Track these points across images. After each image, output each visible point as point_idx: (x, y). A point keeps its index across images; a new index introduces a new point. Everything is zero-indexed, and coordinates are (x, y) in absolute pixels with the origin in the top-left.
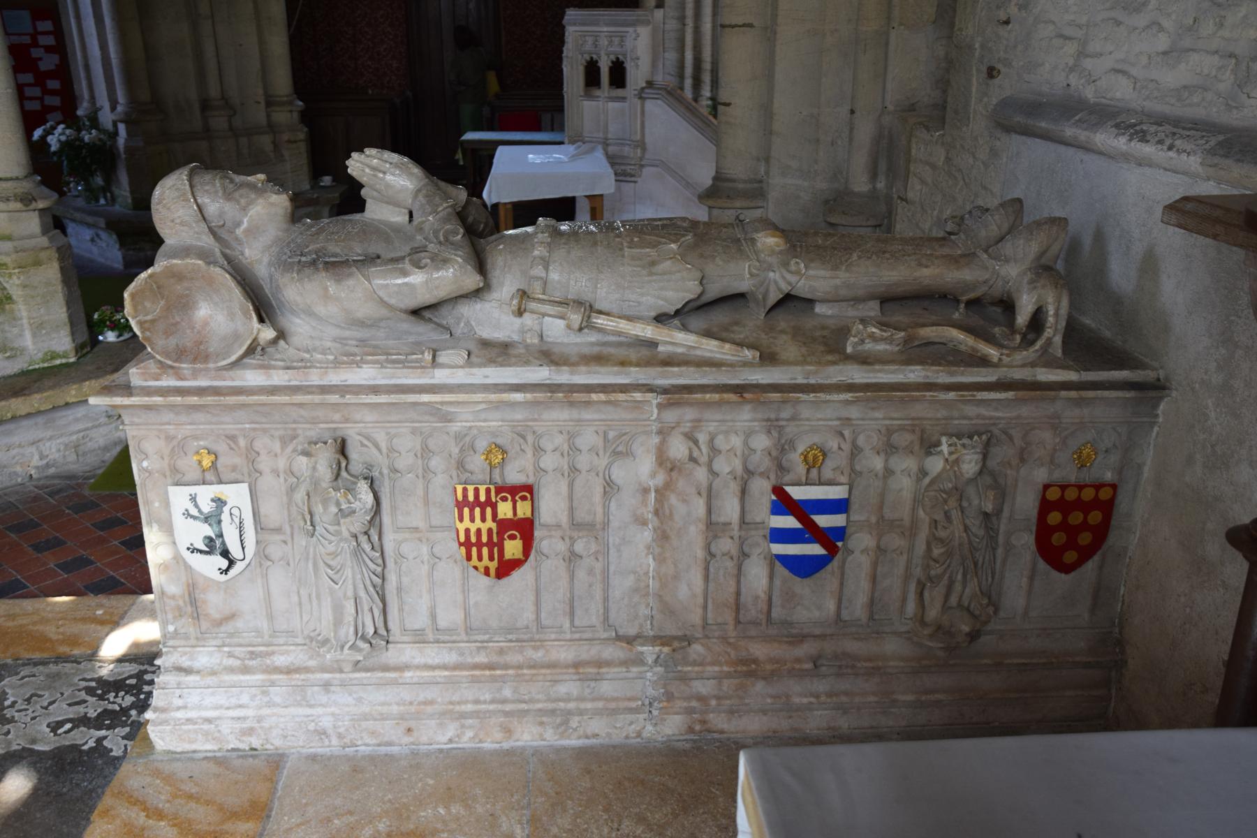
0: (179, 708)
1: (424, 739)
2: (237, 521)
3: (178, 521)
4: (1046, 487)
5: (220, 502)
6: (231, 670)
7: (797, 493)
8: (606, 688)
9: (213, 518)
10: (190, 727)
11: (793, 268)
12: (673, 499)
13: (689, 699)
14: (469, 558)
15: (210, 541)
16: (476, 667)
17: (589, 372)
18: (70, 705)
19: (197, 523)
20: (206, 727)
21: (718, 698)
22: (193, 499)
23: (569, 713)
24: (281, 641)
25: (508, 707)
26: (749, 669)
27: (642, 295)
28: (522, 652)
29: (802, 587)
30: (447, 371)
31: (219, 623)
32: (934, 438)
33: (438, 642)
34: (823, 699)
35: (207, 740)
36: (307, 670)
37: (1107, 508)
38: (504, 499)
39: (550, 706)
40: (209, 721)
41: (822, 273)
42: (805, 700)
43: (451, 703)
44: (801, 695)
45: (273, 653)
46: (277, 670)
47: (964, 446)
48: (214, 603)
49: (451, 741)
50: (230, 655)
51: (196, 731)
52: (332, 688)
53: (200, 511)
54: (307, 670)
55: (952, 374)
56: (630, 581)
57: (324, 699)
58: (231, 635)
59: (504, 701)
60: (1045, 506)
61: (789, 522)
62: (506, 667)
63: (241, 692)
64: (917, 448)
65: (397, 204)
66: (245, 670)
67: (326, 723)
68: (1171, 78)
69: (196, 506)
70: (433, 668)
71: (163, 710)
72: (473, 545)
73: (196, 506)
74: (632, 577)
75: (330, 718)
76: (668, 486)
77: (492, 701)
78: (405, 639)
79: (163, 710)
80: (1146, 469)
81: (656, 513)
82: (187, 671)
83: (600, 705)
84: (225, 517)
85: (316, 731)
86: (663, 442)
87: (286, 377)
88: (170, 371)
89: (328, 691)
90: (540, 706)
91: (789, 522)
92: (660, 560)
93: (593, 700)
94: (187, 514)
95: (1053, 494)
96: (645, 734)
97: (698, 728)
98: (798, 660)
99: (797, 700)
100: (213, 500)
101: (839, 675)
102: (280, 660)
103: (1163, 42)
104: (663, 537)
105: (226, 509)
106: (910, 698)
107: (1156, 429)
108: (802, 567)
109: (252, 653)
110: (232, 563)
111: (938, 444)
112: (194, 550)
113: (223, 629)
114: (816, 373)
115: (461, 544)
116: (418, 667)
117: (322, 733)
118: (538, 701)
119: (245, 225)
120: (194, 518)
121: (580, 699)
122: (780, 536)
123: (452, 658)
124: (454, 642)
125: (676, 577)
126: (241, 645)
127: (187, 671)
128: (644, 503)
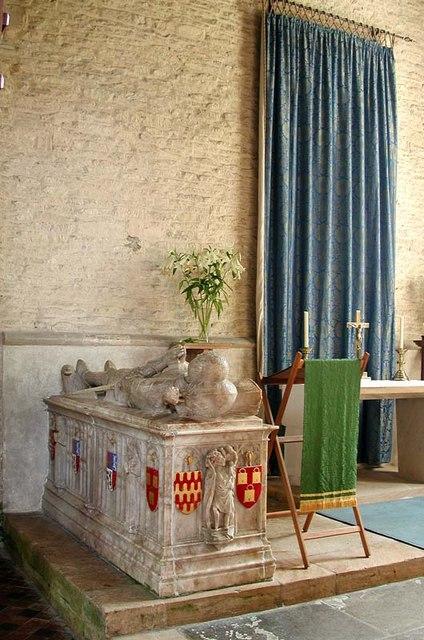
68: (91, 323)
103: (84, 315)
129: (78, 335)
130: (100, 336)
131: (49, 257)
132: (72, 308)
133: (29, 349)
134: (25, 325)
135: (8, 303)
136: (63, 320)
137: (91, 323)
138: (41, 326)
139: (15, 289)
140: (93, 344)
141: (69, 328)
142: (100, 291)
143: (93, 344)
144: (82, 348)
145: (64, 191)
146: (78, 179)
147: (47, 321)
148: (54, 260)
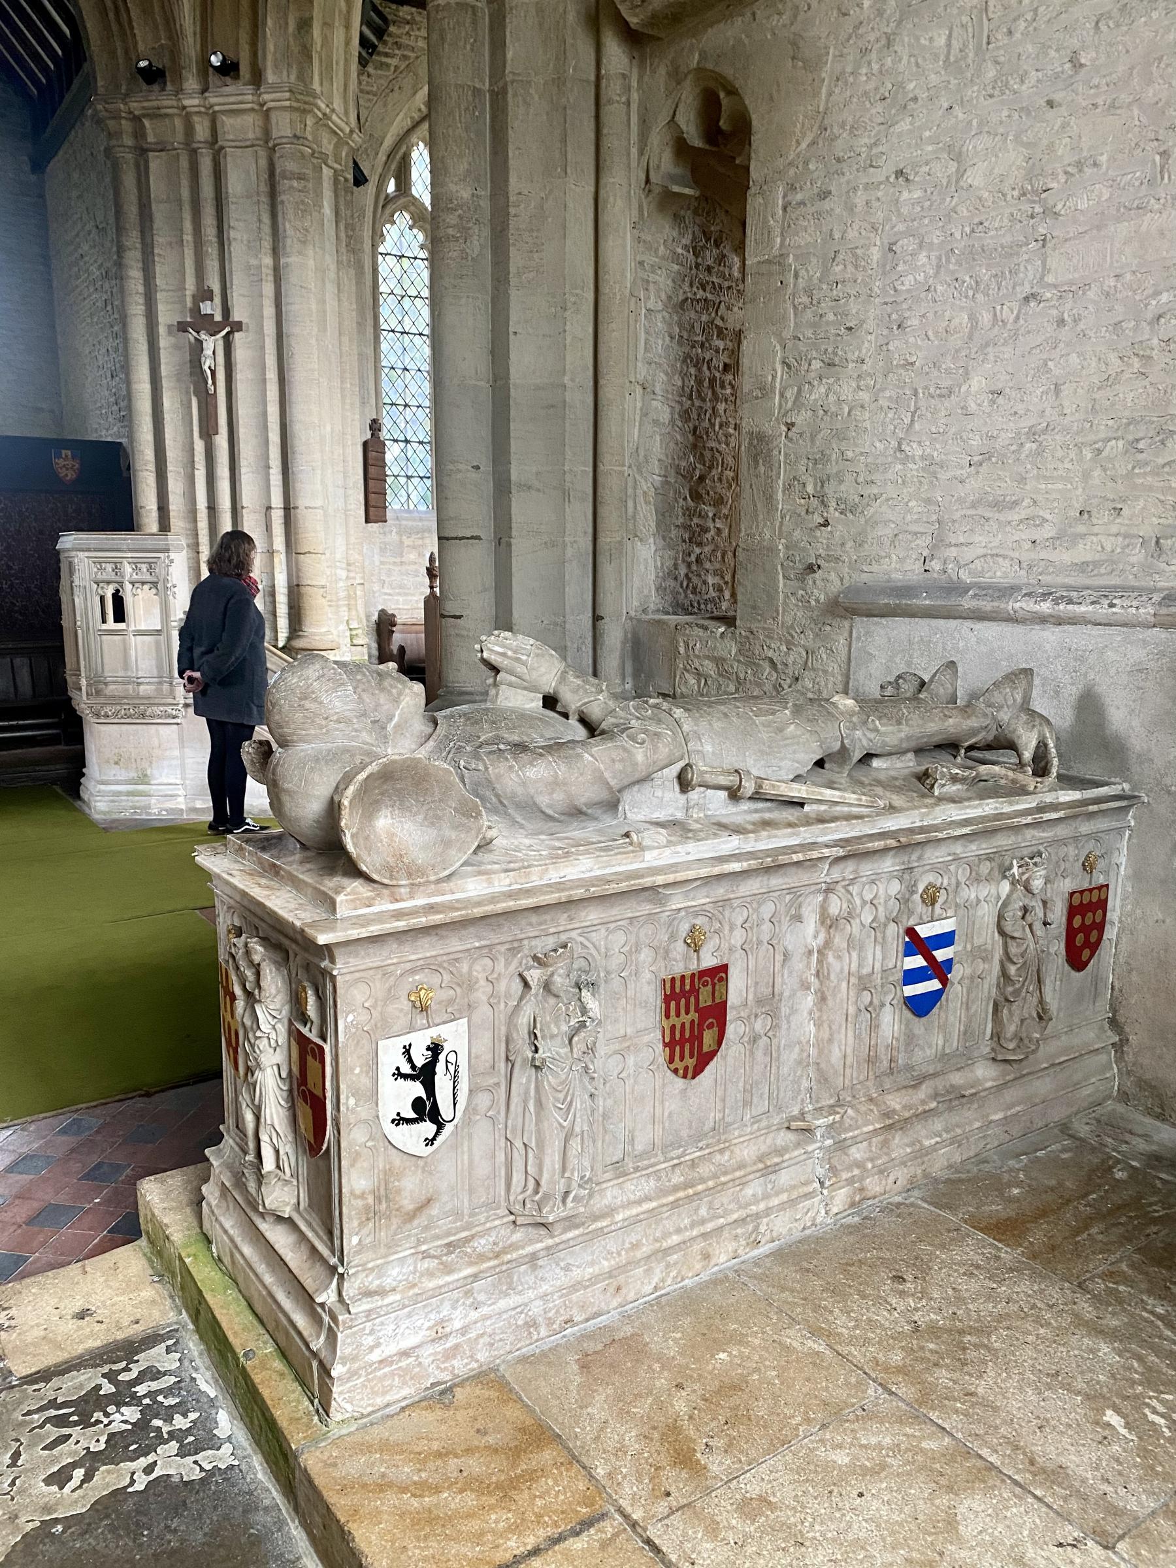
0: (371, 1349)
1: (631, 1296)
2: (451, 1068)
3: (387, 1083)
4: (1072, 894)
5: (435, 1049)
6: (430, 1274)
7: (924, 931)
8: (784, 1178)
9: (426, 1075)
10: (387, 1369)
11: (871, 726)
12: (831, 958)
13: (849, 1168)
14: (671, 1061)
15: (418, 1104)
16: (676, 1188)
17: (769, 837)
18: (49, 1447)
19: (409, 1082)
20: (403, 1363)
21: (872, 1160)
22: (407, 1051)
23: (757, 1216)
24: (482, 1218)
25: (709, 1226)
26: (893, 1125)
27: (782, 759)
28: (710, 1160)
29: (919, 1025)
30: (655, 852)
31: (411, 1216)
32: (1007, 863)
33: (637, 1169)
34: (945, 1136)
35: (405, 1383)
36: (514, 1247)
37: (1103, 904)
38: (705, 984)
39: (742, 1213)
40: (405, 1354)
41: (890, 728)
42: (933, 1142)
43: (656, 1240)
44: (927, 1137)
45: (473, 1237)
46: (482, 1258)
47: (1035, 864)
48: (410, 1187)
49: (656, 1289)
50: (426, 1255)
51: (392, 1374)
52: (540, 1262)
53: (413, 1067)
54: (514, 1247)
55: (1011, 804)
56: (795, 1054)
57: (530, 1279)
58: (426, 1228)
59: (703, 1222)
60: (1072, 911)
61: (918, 961)
62: (703, 1180)
63: (442, 1301)
64: (996, 873)
65: (533, 689)
66: (448, 1269)
67: (536, 1309)
68: (1065, 557)
69: (410, 1060)
70: (639, 1202)
71: (354, 1358)
72: (688, 1040)
73: (410, 1060)
74: (797, 1049)
75: (539, 1303)
76: (827, 944)
77: (693, 1225)
78: (607, 1176)
79: (354, 1358)
80: (1122, 868)
81: (818, 975)
82: (381, 1292)
83: (784, 1197)
84: (440, 1068)
85: (526, 1323)
86: (825, 900)
87: (507, 881)
88: (386, 892)
89: (535, 1268)
90: (735, 1216)
91: (918, 961)
92: (819, 1025)
93: (777, 1194)
94: (399, 1074)
95: (1076, 900)
96: (819, 1220)
97: (857, 1198)
98: (923, 1102)
99: (927, 1143)
100: (428, 1049)
101: (950, 1109)
102: (482, 1244)
103: (1048, 531)
104: (822, 999)
105: (442, 1057)
106: (999, 1116)
107: (1127, 833)
108: (921, 1006)
109: (449, 1245)
110: (440, 1127)
111: (1010, 867)
112: (399, 1120)
113: (416, 1222)
114: (928, 814)
115: (665, 1045)
116: (624, 1207)
117: (532, 1324)
118: (732, 1211)
119: (396, 720)
120: (405, 1076)
121: (766, 1197)
122: (911, 977)
123: (649, 1186)
124: (652, 1166)
125: (830, 1041)
126: (438, 1237)
127: (381, 1292)
128: (808, 966)
129: (1009, 591)
130: (1060, 604)
131: (967, 376)
132: (1014, 516)
133: (901, 628)
134: (898, 565)
135: (869, 512)
136: (986, 552)
137: (1065, 557)
138: (936, 565)
139: (889, 475)
140: (1043, 620)
141: (1002, 573)
142: (1099, 452)
143: (1043, 620)
144: (1019, 629)
145: (1012, 160)
146: (1050, 104)
147: (953, 552)
148: (977, 383)
